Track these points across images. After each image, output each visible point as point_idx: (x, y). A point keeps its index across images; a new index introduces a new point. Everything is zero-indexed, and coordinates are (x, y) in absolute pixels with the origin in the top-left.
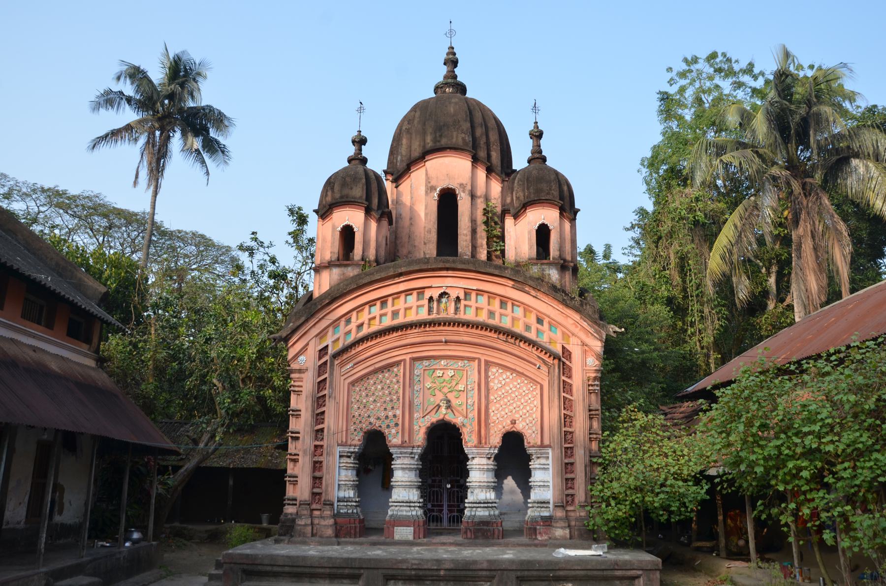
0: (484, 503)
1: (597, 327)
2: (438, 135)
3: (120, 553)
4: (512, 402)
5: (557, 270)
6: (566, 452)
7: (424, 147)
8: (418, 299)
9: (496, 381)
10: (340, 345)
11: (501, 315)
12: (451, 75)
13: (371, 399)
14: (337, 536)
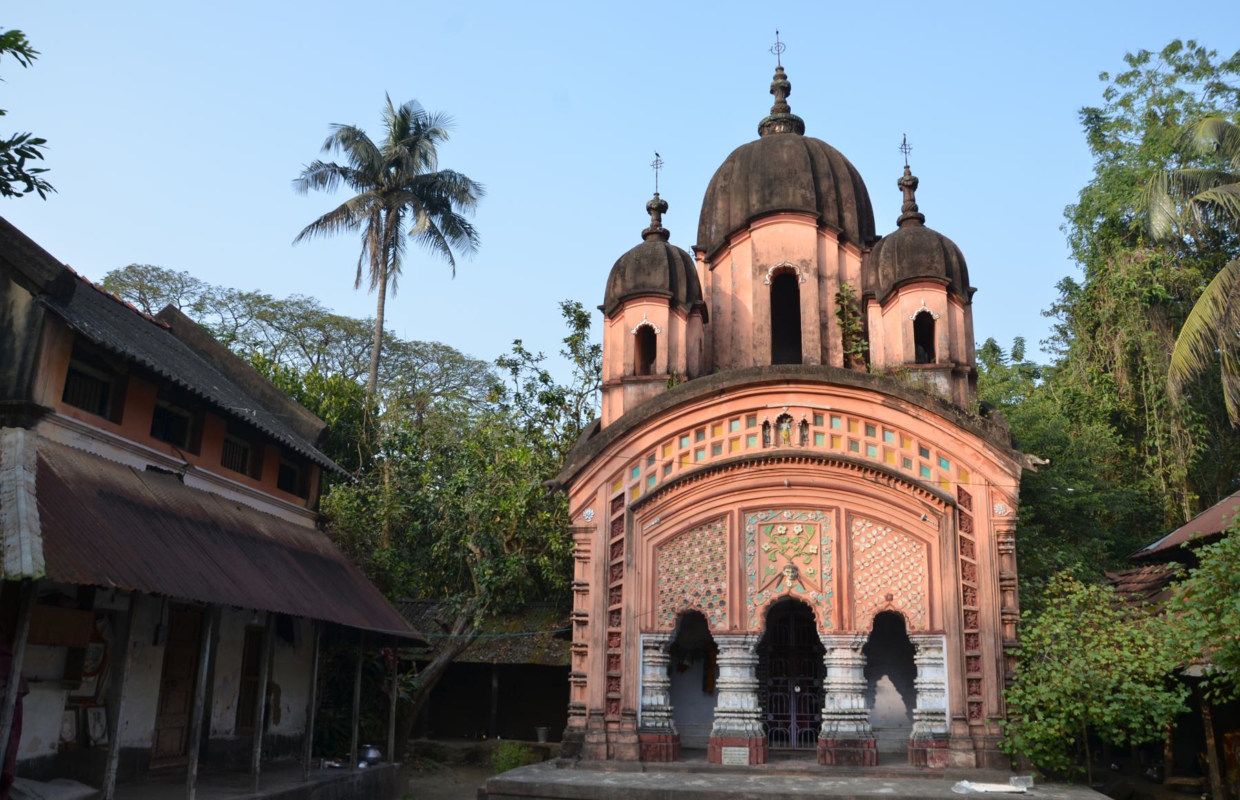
0: (850, 714)
1: (1008, 459)
2: (767, 193)
4: (886, 568)
5: (947, 377)
6: (967, 640)
7: (748, 210)
8: (748, 426)
9: (863, 540)
10: (641, 493)
11: (867, 444)
13: (686, 567)
14: (642, 759)
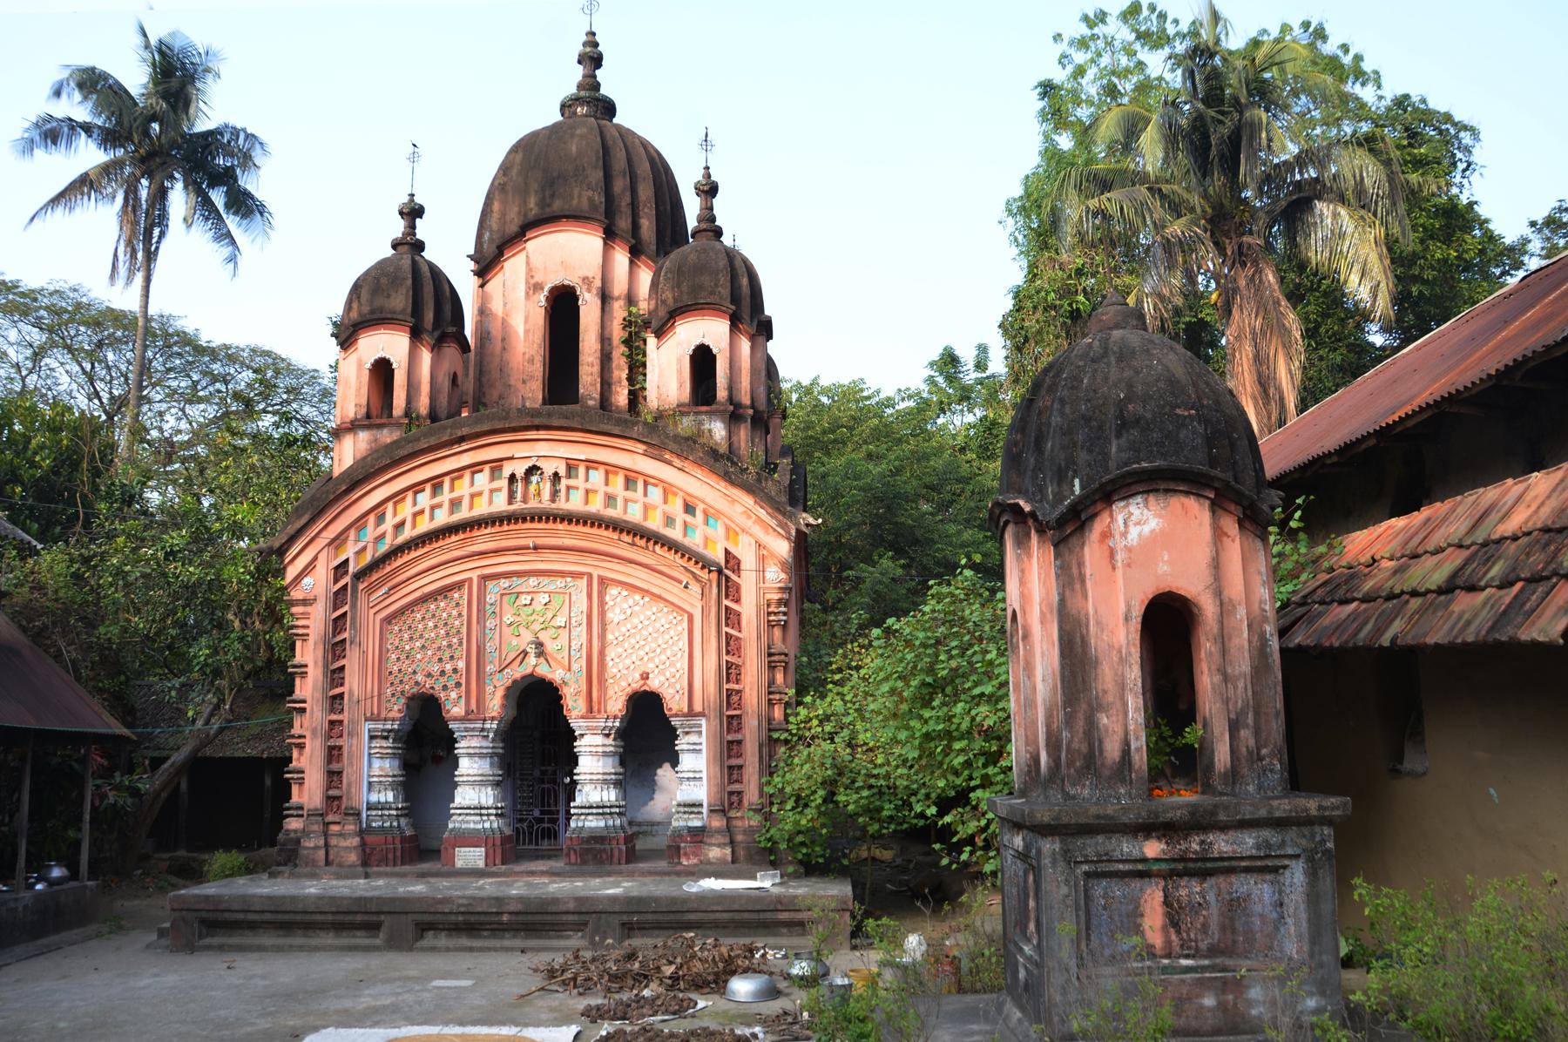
0: (598, 807)
1: (781, 517)
2: (548, 193)
3: (16, 900)
4: (642, 643)
5: (724, 422)
6: (729, 723)
7: (525, 215)
8: (492, 479)
10: (368, 558)
11: (626, 501)
12: (590, 84)
13: (418, 644)
14: (365, 863)
